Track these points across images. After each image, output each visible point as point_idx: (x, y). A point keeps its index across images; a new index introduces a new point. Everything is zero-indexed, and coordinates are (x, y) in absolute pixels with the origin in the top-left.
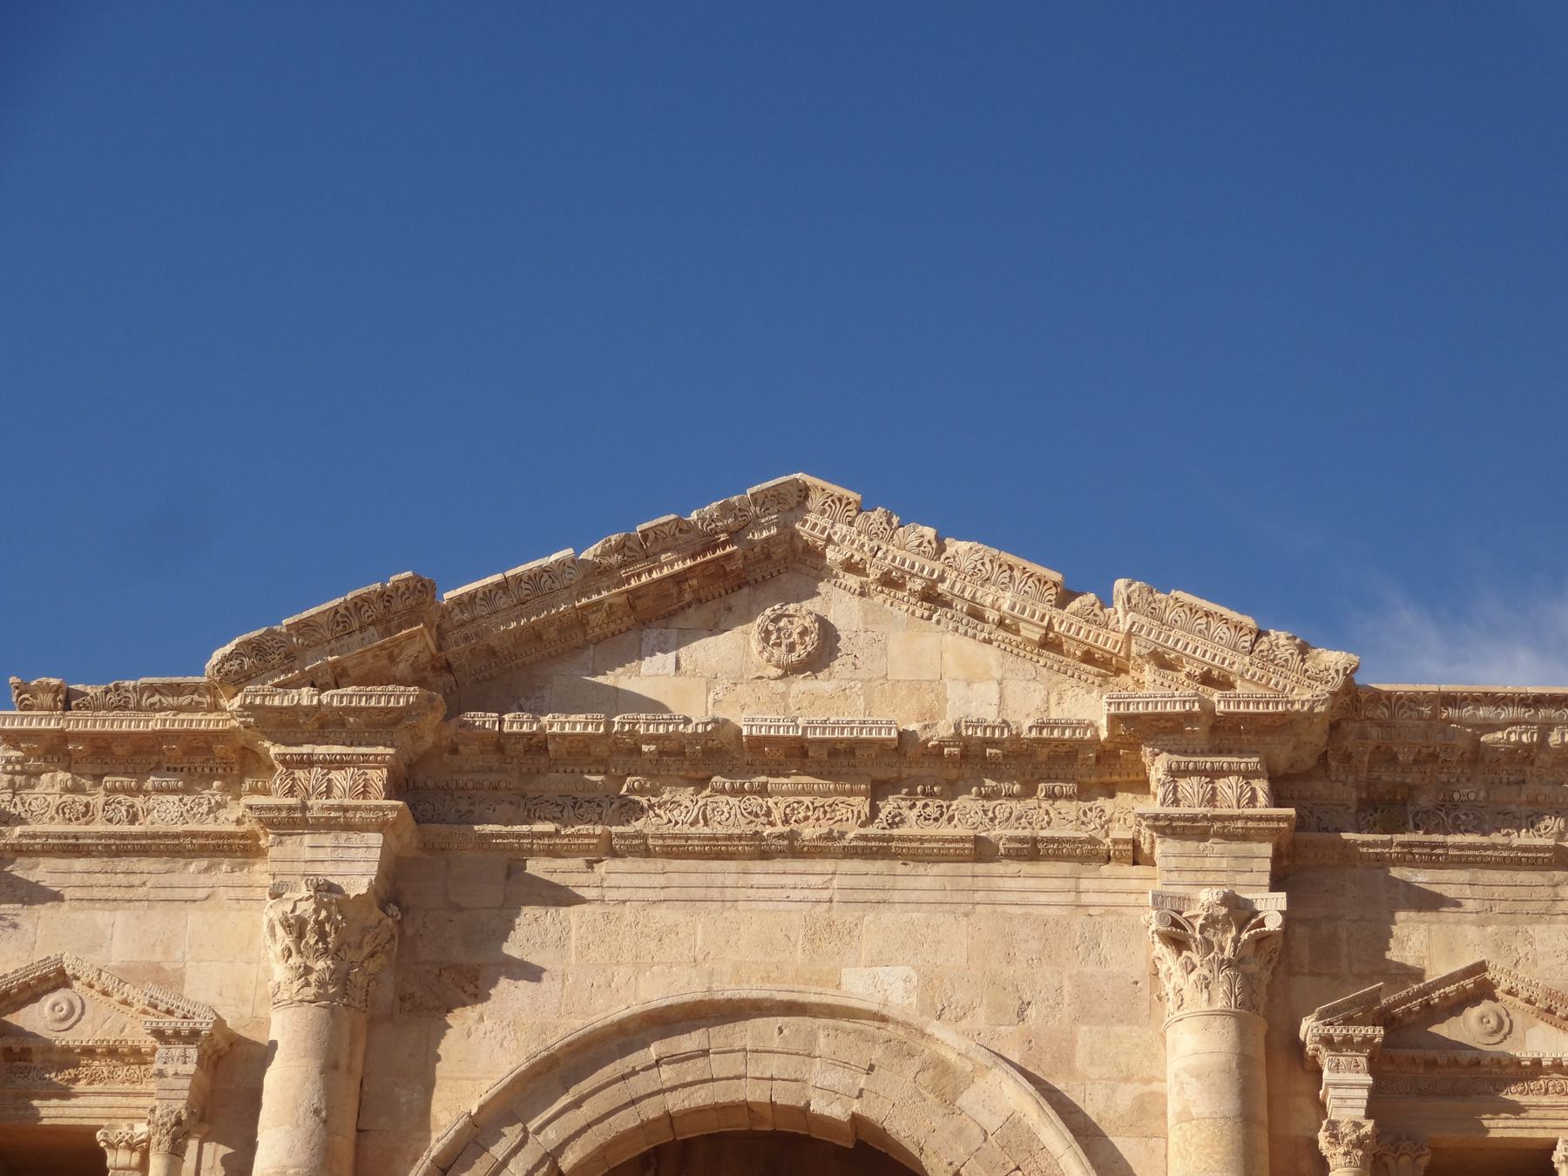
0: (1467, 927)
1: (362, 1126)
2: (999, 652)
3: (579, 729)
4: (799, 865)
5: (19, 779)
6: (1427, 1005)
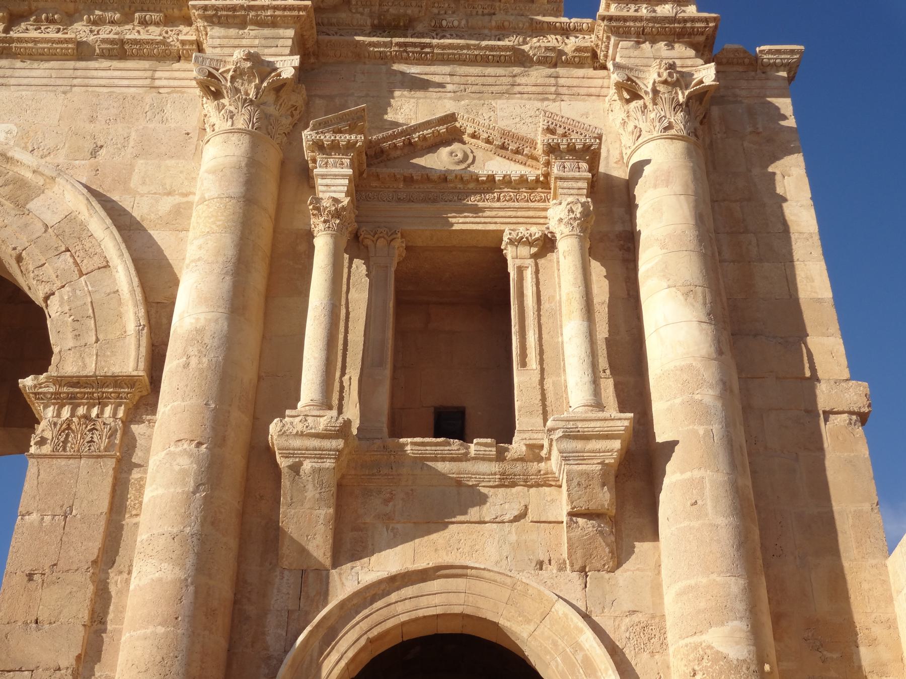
0: (446, 101)
6: (410, 144)
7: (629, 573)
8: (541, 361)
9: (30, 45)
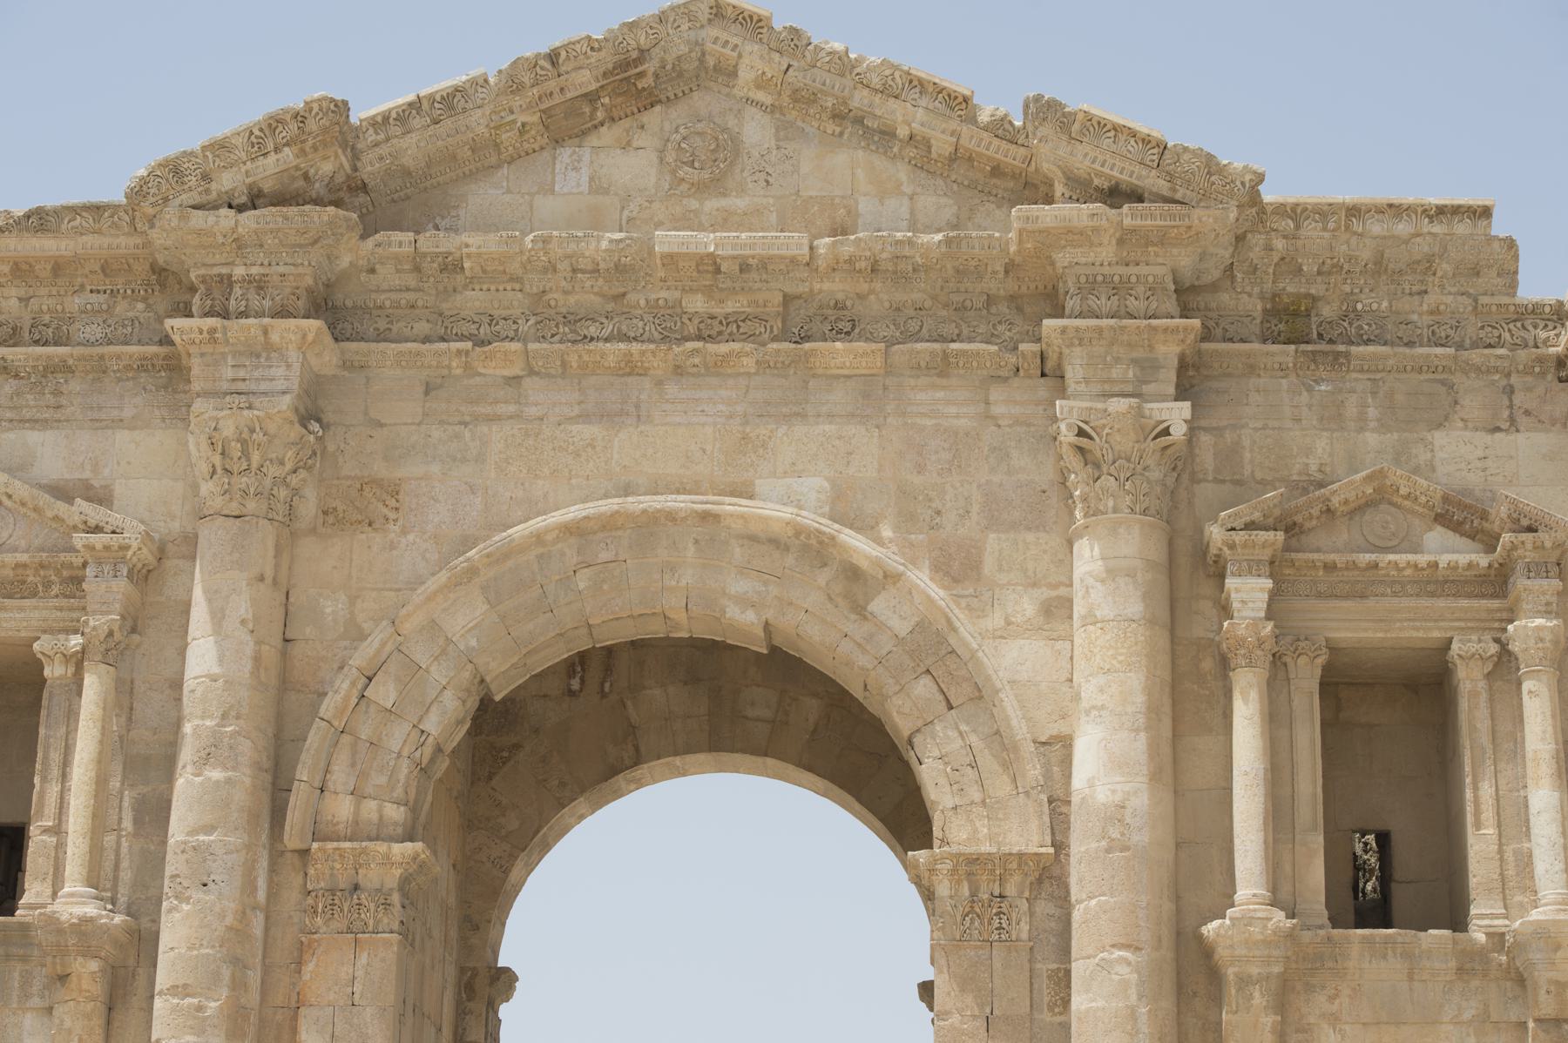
1: (289, 636)
2: (910, 167)
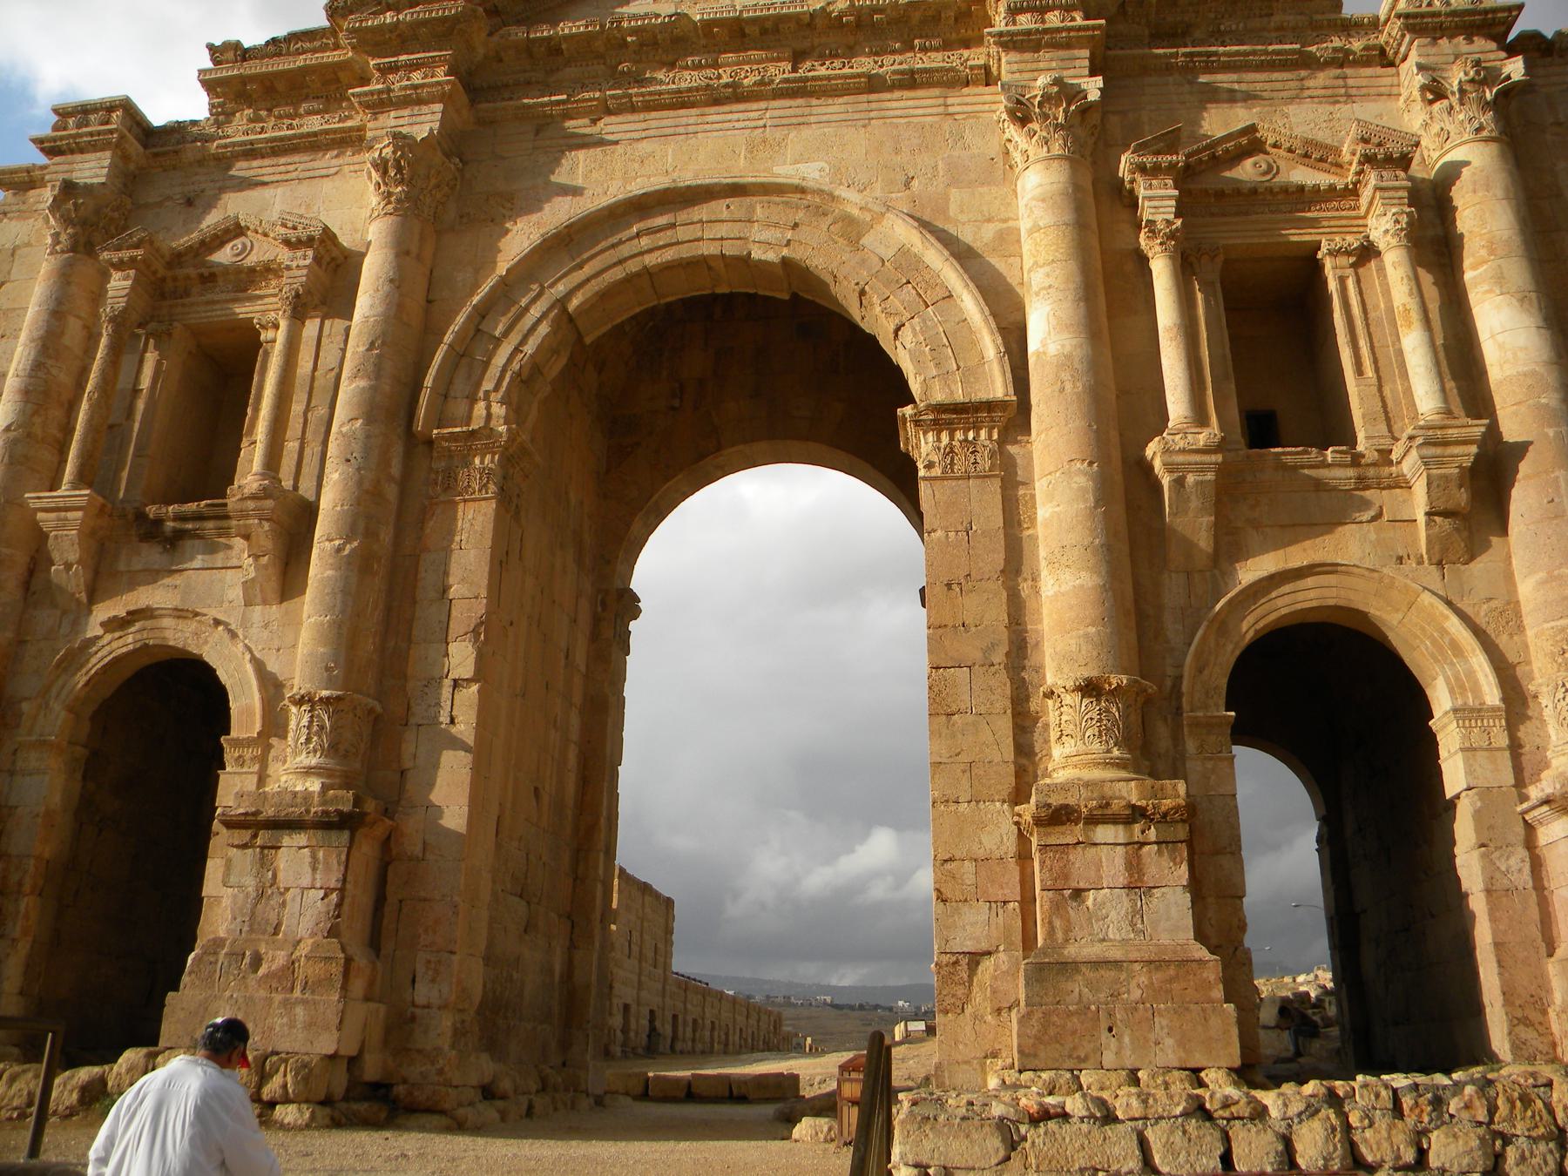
1: (430, 297)
3: (582, 29)
4: (741, 107)
5: (221, 118)
6: (1213, 157)
7: (1482, 565)
8: (1377, 370)
9: (825, 82)
